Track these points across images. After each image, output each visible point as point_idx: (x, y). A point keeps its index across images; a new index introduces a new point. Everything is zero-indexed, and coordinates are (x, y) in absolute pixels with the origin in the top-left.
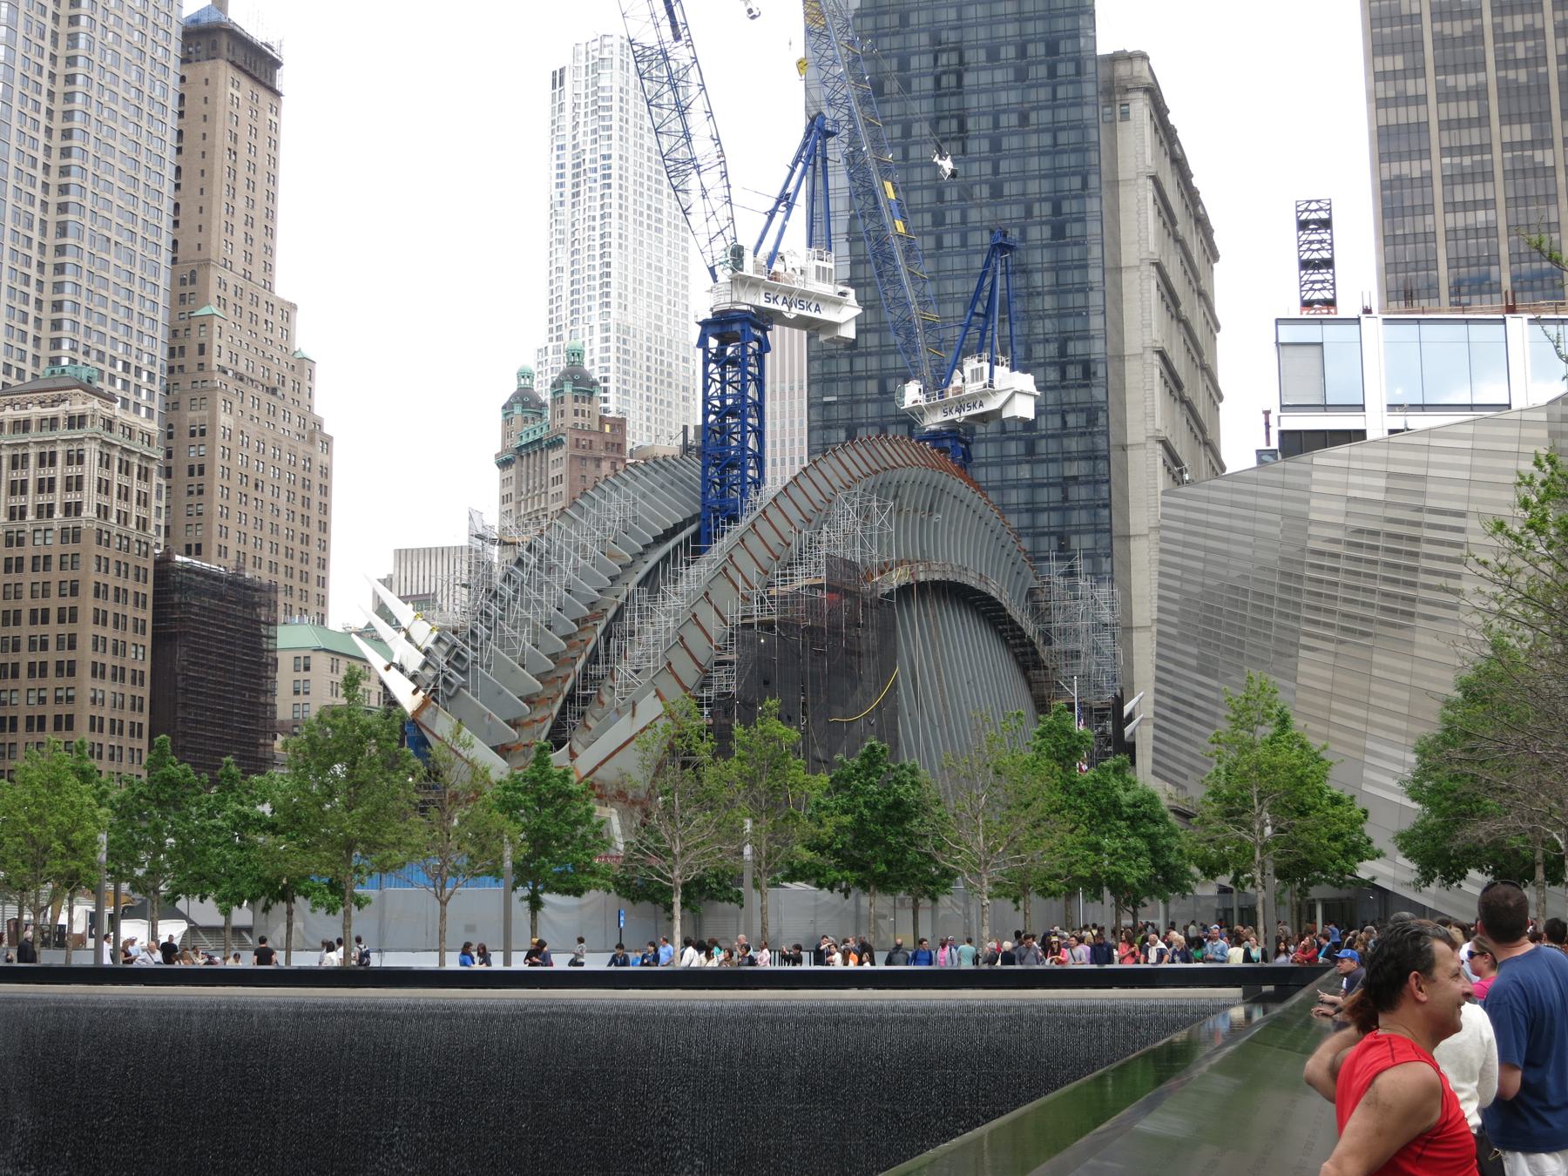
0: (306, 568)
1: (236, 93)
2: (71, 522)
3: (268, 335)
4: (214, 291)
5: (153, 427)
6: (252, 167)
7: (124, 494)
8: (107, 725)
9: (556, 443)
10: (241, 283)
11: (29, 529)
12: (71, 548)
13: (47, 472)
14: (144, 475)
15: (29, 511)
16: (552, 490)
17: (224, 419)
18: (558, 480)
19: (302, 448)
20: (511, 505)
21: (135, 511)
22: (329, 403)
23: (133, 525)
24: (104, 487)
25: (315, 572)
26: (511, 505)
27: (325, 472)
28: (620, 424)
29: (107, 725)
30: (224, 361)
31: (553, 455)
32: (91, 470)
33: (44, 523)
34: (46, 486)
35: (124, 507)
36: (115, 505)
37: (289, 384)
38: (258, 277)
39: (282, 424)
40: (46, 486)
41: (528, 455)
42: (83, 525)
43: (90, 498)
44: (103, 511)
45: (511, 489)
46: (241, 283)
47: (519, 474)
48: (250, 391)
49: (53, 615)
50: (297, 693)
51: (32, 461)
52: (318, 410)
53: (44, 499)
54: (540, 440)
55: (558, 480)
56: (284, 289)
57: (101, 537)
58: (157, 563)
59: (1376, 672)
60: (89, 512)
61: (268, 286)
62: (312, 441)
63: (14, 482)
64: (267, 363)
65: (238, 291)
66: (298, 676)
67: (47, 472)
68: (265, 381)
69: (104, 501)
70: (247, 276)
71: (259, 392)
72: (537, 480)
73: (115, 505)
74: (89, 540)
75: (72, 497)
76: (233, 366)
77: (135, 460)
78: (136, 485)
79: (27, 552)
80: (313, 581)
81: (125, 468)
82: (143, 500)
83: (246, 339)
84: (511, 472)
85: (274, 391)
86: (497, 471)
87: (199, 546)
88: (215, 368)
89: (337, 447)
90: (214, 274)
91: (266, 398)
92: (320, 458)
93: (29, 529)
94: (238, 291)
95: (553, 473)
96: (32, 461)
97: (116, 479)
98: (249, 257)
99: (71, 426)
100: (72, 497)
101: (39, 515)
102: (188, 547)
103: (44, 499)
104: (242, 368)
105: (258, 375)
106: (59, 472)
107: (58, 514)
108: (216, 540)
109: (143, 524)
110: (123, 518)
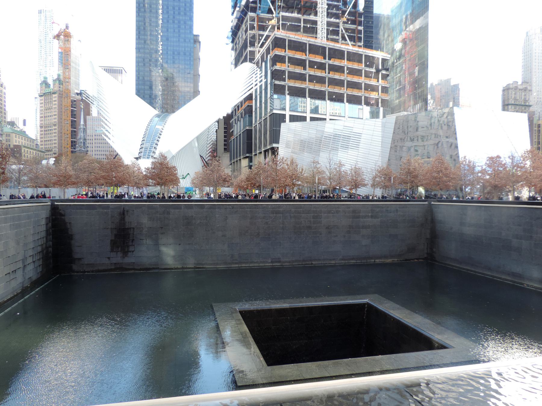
9: (54, 93)
16: (54, 103)
18: (55, 101)
20: (43, 105)
25: (4, 115)
31: (54, 96)
41: (47, 95)
45: (43, 101)
47: (45, 99)
54: (50, 92)
55: (55, 101)
59: (338, 156)
66: (7, 138)
72: (50, 100)
80: (3, 117)
84: (43, 98)
92: (4, 90)
95: (54, 99)
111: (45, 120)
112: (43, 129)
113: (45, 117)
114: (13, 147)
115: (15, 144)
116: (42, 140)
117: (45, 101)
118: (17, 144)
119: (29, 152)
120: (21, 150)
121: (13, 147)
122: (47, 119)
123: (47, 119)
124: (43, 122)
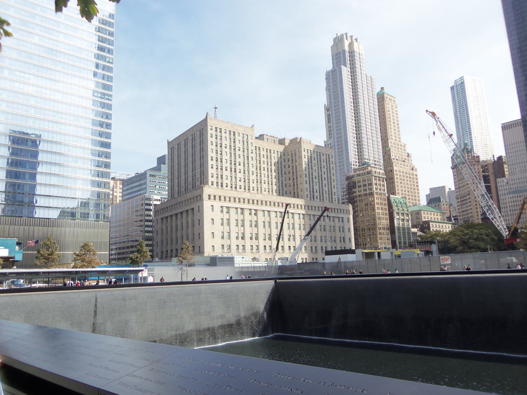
1: (389, 106)
3: (401, 151)
4: (390, 144)
5: (382, 171)
6: (394, 119)
7: (380, 185)
8: (382, 228)
10: (395, 142)
14: (383, 181)
17: (395, 168)
19: (411, 172)
22: (415, 162)
26: (456, 177)
27: (416, 175)
28: (478, 157)
29: (382, 228)
30: (394, 157)
37: (407, 159)
38: (398, 140)
39: (406, 167)
44: (376, 189)
45: (455, 173)
46: (395, 142)
47: (457, 170)
48: (399, 162)
50: (417, 219)
52: (413, 163)
53: (364, 188)
56: (403, 141)
58: (387, 198)
61: (400, 141)
62: (413, 169)
64: (402, 156)
65: (394, 144)
68: (402, 160)
70: (396, 140)
71: (401, 162)
75: (370, 187)
76: (395, 158)
83: (397, 152)
84: (455, 170)
85: (404, 161)
86: (452, 170)
88: (392, 159)
89: (418, 170)
90: (389, 141)
91: (403, 163)
92: (415, 173)
94: (394, 144)
98: (395, 137)
99: (368, 174)
104: (397, 158)
105: (400, 159)
107: (368, 190)
108: (397, 191)
109: (384, 190)
111: (459, 191)
112: (459, 200)
113: (459, 188)
114: (422, 223)
115: (424, 220)
116: (459, 211)
117: (457, 173)
118: (426, 220)
119: (441, 226)
120: (429, 225)
121: (422, 223)
122: (460, 190)
123: (460, 190)
124: (458, 193)
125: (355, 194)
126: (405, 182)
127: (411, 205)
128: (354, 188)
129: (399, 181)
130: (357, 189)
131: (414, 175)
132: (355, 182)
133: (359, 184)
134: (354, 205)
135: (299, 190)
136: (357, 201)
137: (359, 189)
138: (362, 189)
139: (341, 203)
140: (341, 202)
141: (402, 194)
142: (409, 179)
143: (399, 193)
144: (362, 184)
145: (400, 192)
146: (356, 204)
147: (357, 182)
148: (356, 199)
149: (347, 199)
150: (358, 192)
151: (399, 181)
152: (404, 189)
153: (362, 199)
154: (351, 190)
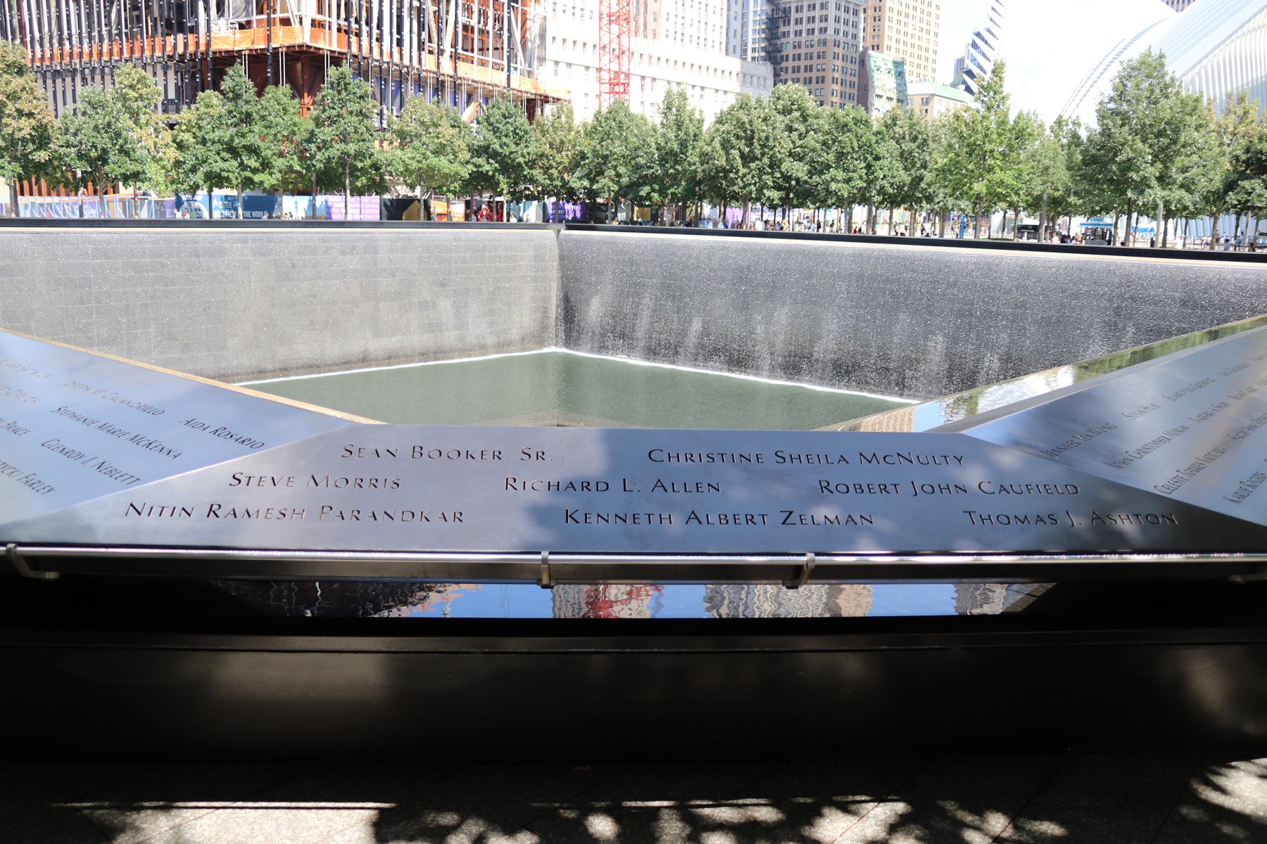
0: (927, 55)
2: (822, 37)
7: (846, 23)
11: (803, 41)
12: (822, 49)
13: (811, 14)
15: (804, 32)
21: (851, 30)
23: (850, 37)
24: (837, 20)
32: (832, 12)
33: (811, 37)
34: (811, 20)
35: (846, 29)
36: (842, 28)
40: (811, 20)
42: (828, 38)
43: (831, 25)
44: (837, 32)
49: (814, 80)
51: (805, 8)
57: (837, 44)
60: (830, 31)
63: (797, 19)
67: (811, 14)
69: (837, 26)
73: (842, 28)
74: (830, 44)
75: (823, 25)
77: (851, 7)
78: (851, 18)
79: (803, 51)
81: (847, 10)
82: (855, 25)
87: (878, 46)
93: (803, 41)
96: (805, 8)
97: (843, 15)
100: (823, 25)
101: (808, 34)
102: (873, 46)
103: (811, 26)
106: (817, 13)
107: (816, 33)
108: (886, 42)
109: (855, 36)
110: (846, 34)
125: (783, 40)
126: (910, 20)
127: (914, 78)
128: (784, 25)
129: (895, 16)
130: (792, 28)
131: (934, 6)
132: (790, 8)
133: (799, 15)
134: (778, 67)
135: (650, 18)
136: (787, 56)
137: (798, 27)
138: (804, 27)
139: (749, 59)
140: (750, 54)
141: (898, 51)
142: (918, 14)
143: (889, 48)
144: (805, 14)
145: (893, 45)
146: (784, 64)
147: (793, 10)
148: (784, 53)
149: (764, 49)
150: (792, 35)
151: (895, 16)
152: (902, 38)
153: (799, 55)
154: (778, 28)
